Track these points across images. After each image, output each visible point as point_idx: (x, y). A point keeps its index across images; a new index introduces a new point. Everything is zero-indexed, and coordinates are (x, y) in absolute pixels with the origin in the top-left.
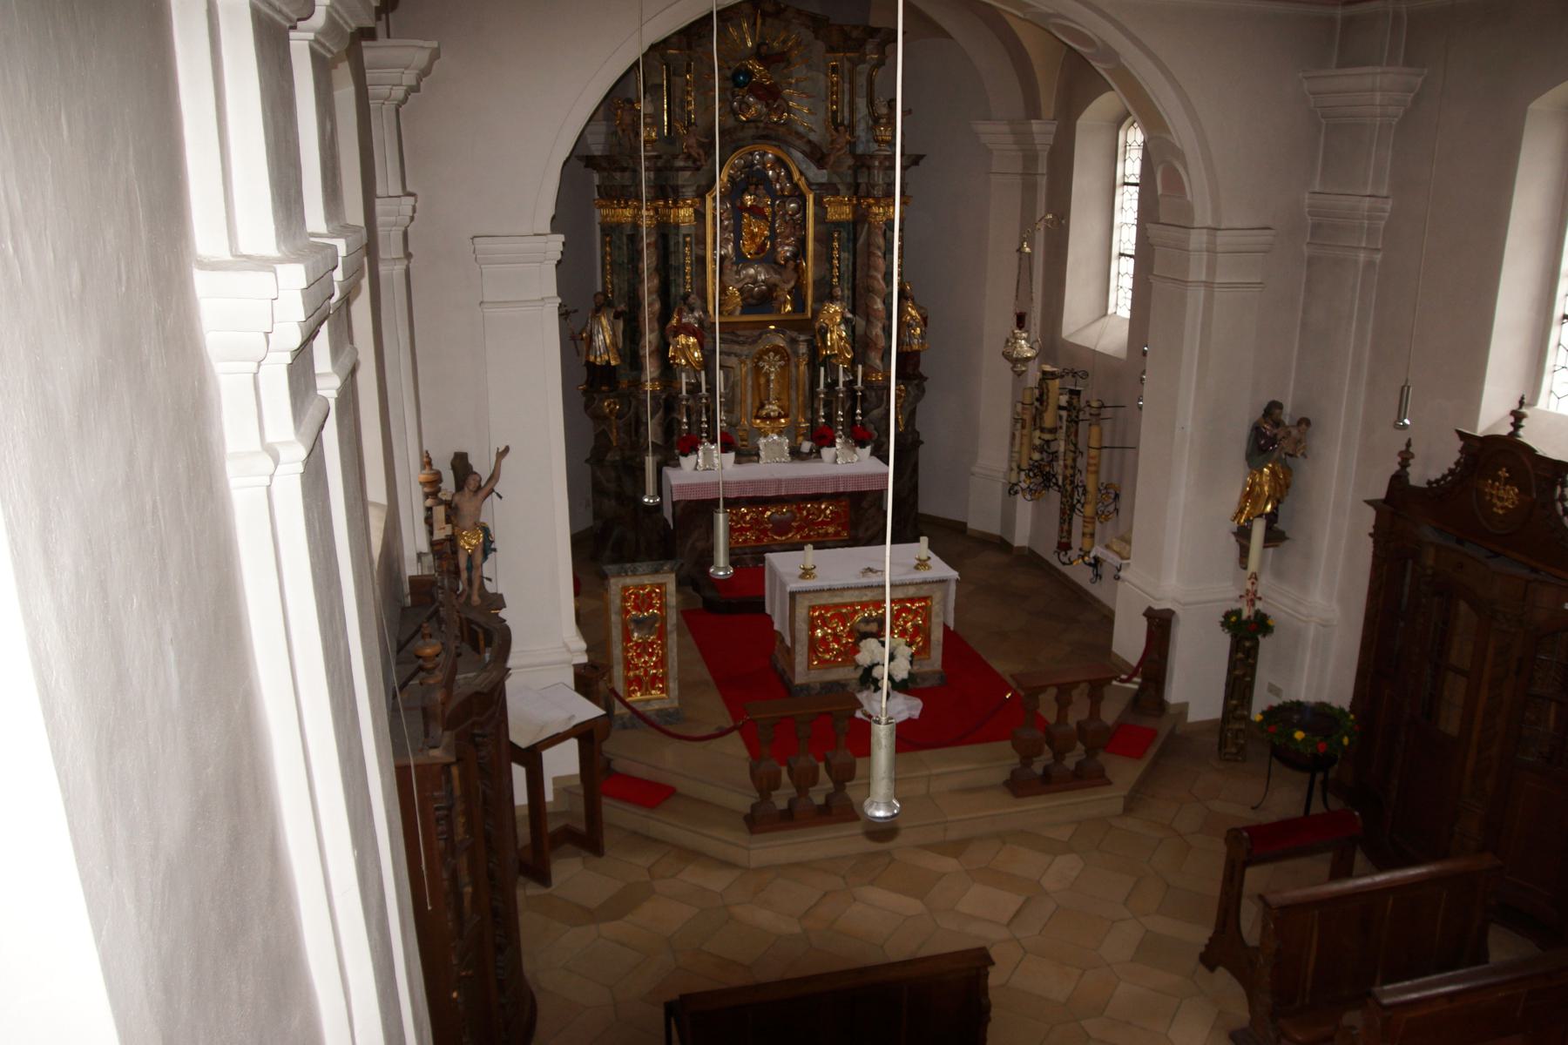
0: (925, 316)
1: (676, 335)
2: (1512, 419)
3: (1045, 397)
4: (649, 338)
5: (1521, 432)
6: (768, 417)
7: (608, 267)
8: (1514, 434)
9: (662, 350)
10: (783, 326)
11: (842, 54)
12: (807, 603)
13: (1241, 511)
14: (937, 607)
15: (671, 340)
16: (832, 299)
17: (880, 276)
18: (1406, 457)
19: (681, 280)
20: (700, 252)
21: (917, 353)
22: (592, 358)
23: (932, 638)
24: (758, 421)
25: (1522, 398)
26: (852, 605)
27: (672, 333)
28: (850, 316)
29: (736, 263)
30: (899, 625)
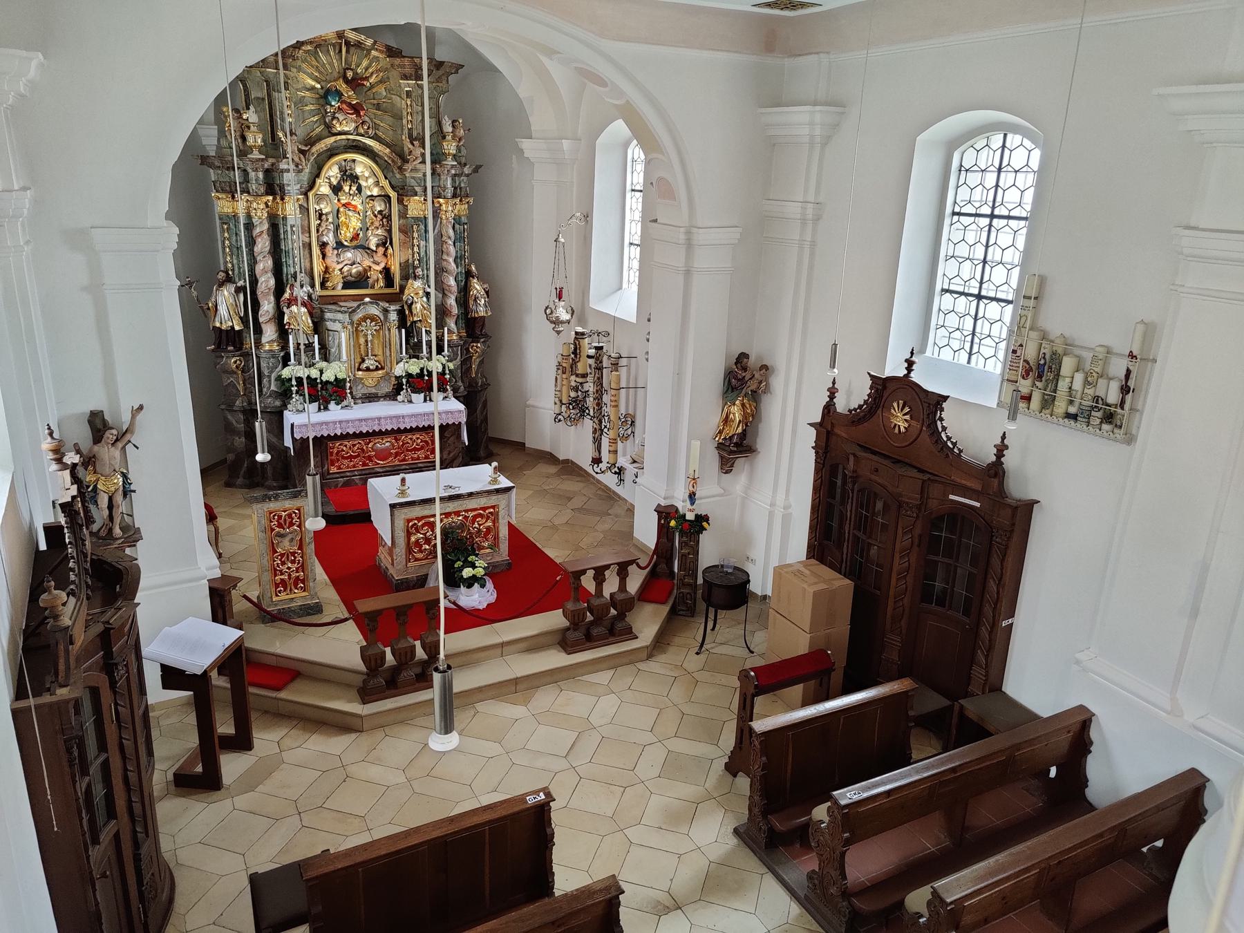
2: (906, 365)
3: (578, 351)
5: (912, 374)
6: (368, 369)
7: (228, 250)
8: (907, 376)
9: (279, 315)
10: (376, 298)
11: (414, 82)
13: (720, 432)
15: (285, 309)
16: (415, 277)
17: (451, 260)
18: (832, 392)
22: (218, 325)
23: (501, 535)
24: (360, 373)
25: (913, 350)
29: (337, 248)
30: (475, 527)
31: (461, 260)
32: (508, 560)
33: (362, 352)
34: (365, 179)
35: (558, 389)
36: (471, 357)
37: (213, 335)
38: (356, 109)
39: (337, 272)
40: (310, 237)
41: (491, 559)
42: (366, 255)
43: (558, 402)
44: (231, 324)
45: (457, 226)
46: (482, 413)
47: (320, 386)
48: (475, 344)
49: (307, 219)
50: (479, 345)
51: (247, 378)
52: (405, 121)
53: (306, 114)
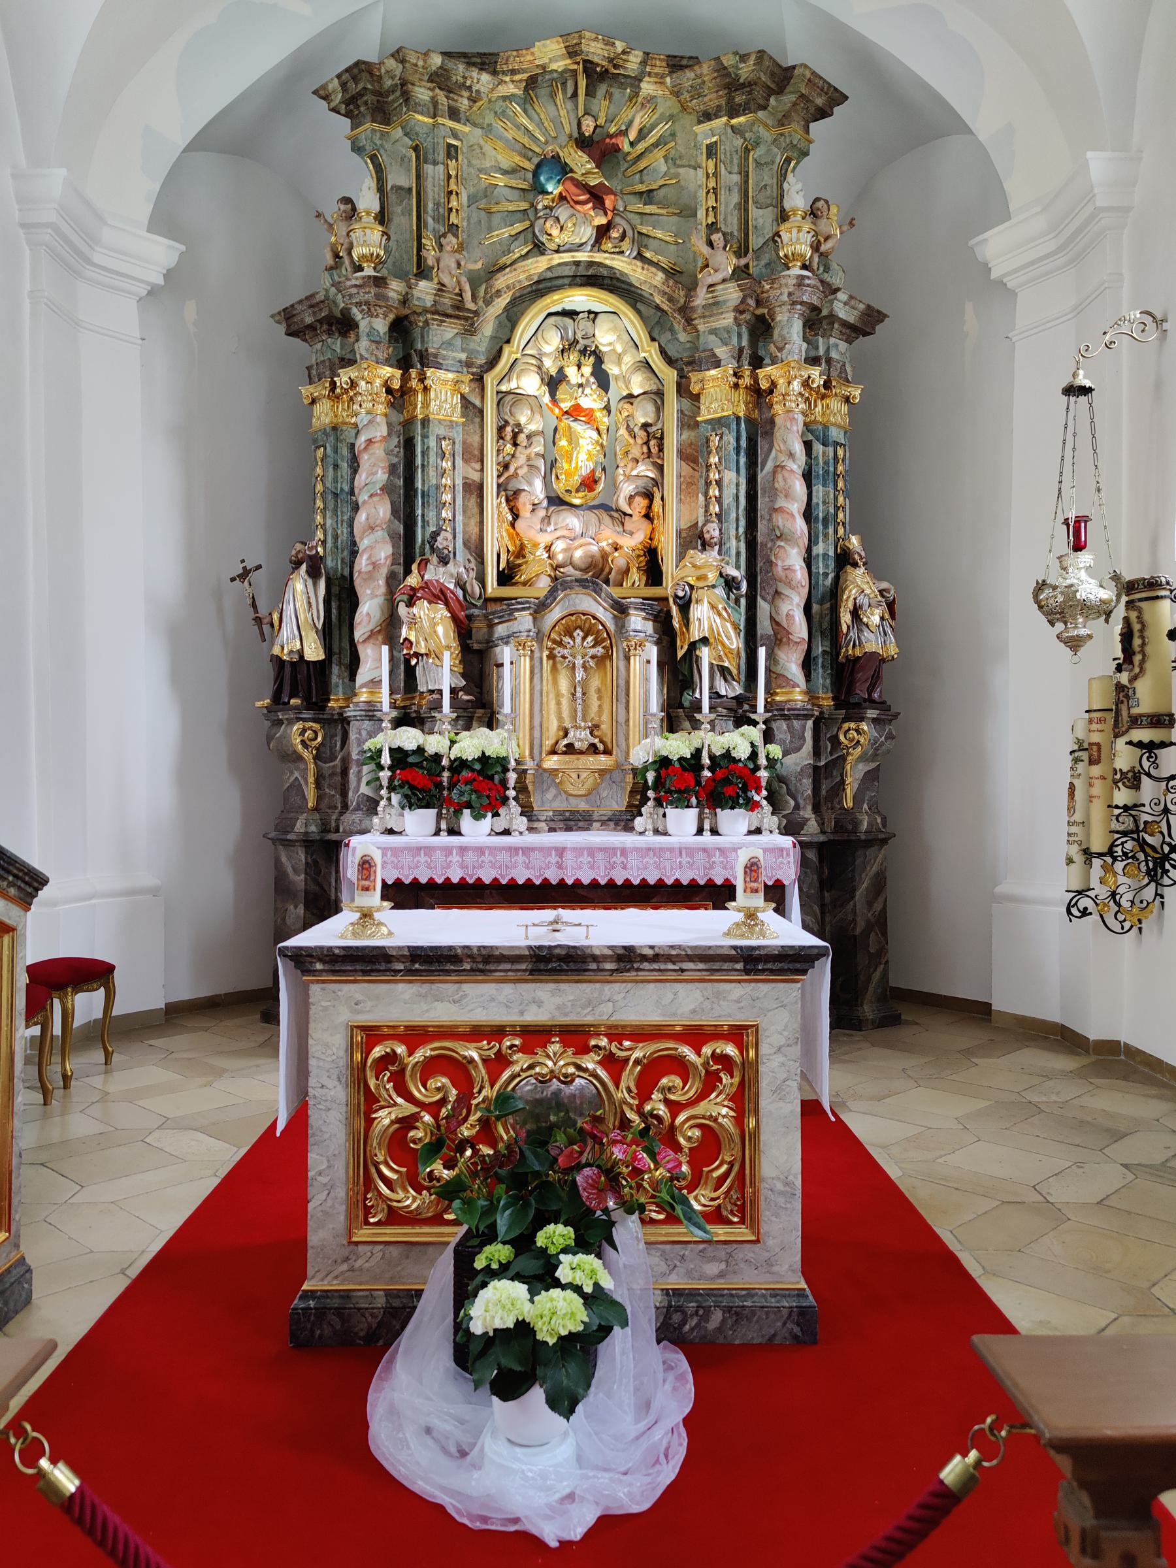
0: (890, 596)
1: (410, 604)
3: (1137, 642)
4: (369, 610)
9: (390, 627)
11: (724, 119)
12: (345, 1016)
14: (779, 1059)
15: (402, 610)
16: (705, 546)
19: (431, 515)
20: (475, 476)
21: (876, 661)
22: (276, 650)
24: (555, 757)
26: (497, 1032)
27: (405, 597)
28: (734, 572)
31: (826, 526)
32: (800, 1293)
33: (566, 714)
34: (614, 358)
35: (1078, 817)
36: (843, 758)
37: (269, 672)
38: (596, 197)
39: (541, 553)
40: (482, 470)
41: (722, 1275)
42: (607, 520)
43: (1079, 858)
44: (298, 646)
45: (818, 448)
46: (870, 904)
47: (446, 774)
48: (853, 725)
49: (478, 431)
50: (864, 726)
51: (327, 773)
52: (701, 214)
53: (496, 219)
